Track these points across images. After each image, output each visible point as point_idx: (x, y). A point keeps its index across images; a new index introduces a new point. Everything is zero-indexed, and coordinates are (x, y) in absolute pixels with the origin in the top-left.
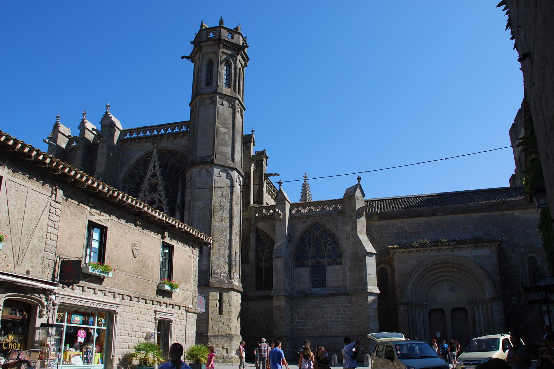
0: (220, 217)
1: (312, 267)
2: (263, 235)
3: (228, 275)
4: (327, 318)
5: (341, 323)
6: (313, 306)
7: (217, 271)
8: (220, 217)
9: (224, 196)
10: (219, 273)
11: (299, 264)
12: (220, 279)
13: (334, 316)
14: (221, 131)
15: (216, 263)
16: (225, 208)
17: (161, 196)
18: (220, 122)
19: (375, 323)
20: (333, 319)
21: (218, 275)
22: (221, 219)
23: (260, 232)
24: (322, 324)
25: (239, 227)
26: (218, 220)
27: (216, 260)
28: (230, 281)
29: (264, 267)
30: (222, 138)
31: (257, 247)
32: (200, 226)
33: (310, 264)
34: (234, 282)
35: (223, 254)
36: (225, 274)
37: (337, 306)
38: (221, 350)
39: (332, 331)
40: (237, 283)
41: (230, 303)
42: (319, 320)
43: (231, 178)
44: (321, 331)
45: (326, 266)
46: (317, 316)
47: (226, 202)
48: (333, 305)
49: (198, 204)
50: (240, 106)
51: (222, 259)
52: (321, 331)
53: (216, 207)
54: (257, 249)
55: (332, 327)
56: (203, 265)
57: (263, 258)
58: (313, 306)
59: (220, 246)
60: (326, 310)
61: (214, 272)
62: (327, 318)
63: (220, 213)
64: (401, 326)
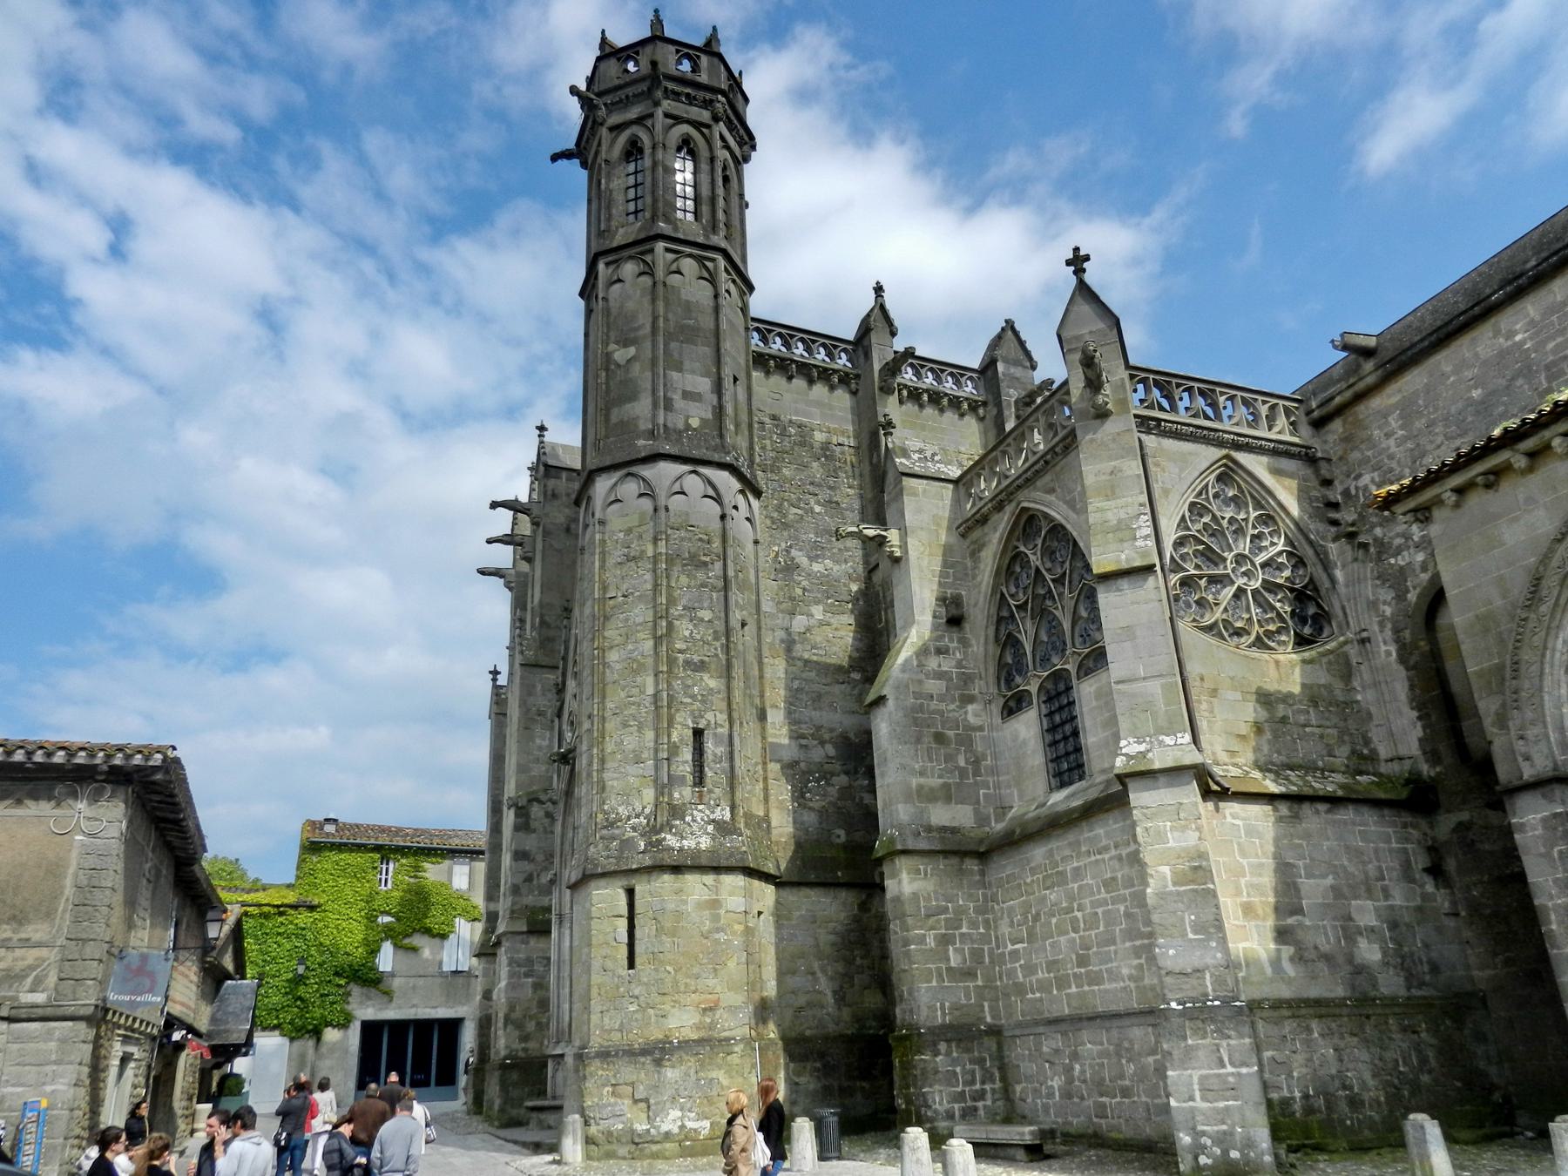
1: (1044, 702)
4: (1082, 925)
5: (1128, 944)
6: (1041, 876)
11: (1012, 704)
12: (622, 841)
13: (1104, 913)
18: (613, 338)
19: (1195, 932)
20: (1101, 929)
24: (1074, 957)
25: (716, 639)
33: (1033, 688)
36: (642, 818)
37: (1104, 860)
38: (626, 1108)
39: (1107, 986)
41: (660, 919)
42: (1062, 939)
43: (649, 493)
44: (1074, 989)
45: (1074, 681)
46: (1054, 921)
48: (1093, 858)
50: (688, 250)
51: (633, 769)
52: (1074, 989)
53: (612, 602)
55: (1103, 967)
58: (1041, 876)
59: (625, 725)
60: (1076, 886)
61: (607, 820)
62: (1082, 925)
64: (1554, 927)
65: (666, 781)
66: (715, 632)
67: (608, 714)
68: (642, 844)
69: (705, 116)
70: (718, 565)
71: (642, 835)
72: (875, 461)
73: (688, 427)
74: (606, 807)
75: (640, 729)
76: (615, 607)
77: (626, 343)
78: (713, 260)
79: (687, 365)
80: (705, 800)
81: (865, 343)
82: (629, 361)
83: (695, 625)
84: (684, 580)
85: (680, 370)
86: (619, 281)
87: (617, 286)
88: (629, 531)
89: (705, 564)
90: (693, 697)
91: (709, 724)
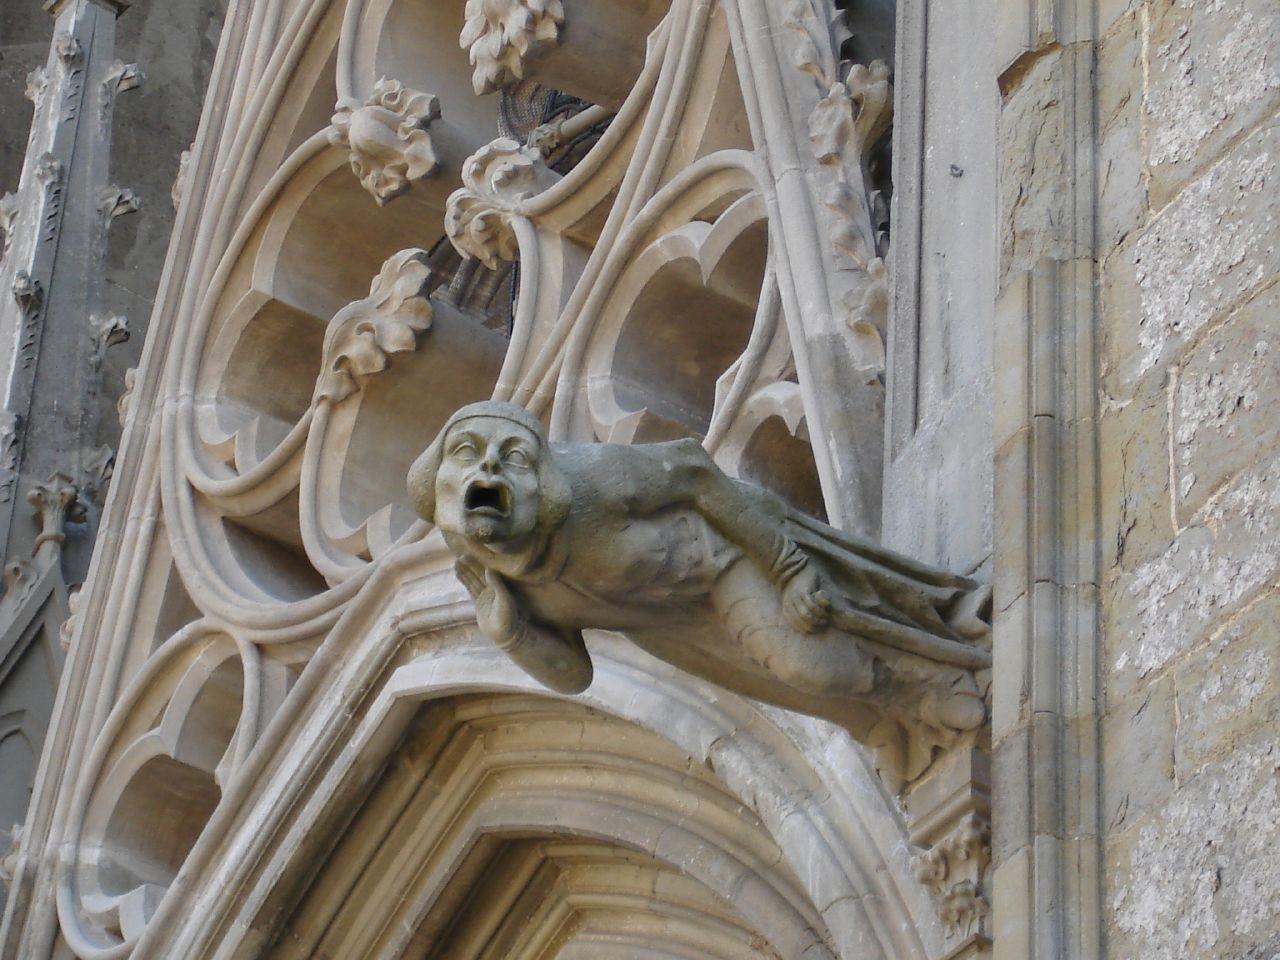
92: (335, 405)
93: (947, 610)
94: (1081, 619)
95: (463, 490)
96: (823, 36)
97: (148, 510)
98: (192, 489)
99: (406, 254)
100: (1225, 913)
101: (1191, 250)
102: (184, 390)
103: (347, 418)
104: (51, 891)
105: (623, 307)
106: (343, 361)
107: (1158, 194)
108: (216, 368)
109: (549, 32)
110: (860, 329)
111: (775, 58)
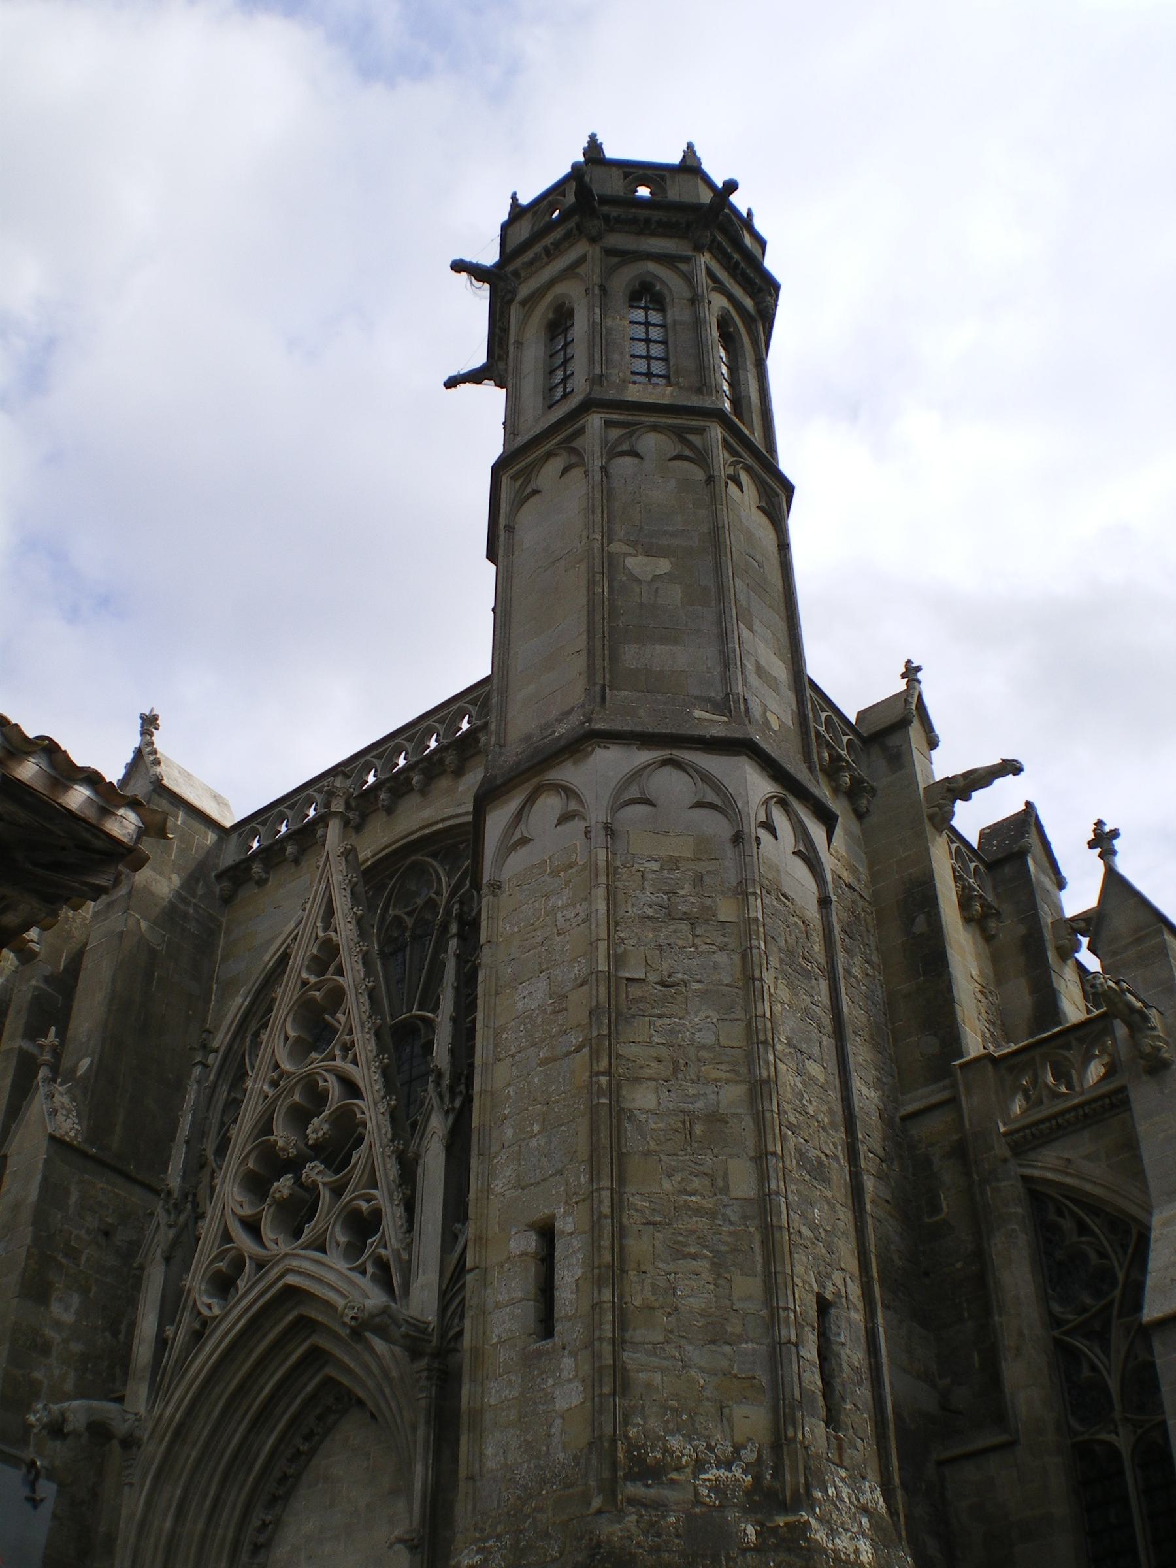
0: (664, 1052)
2: (1083, 1228)
3: (757, 1479)
7: (666, 1451)
8: (664, 1052)
9: (686, 917)
10: (679, 1469)
14: (636, 571)
15: (649, 1386)
16: (698, 986)
17: (355, 1056)
21: (672, 1481)
22: (675, 1062)
23: (1060, 1213)
25: (833, 1124)
26: (653, 1069)
27: (655, 1361)
28: (781, 1521)
29: (1126, 1455)
30: (642, 605)
31: (1055, 1322)
32: (534, 1143)
34: (819, 1534)
35: (704, 1314)
40: (864, 1546)
47: (703, 948)
49: (520, 1006)
50: (750, 461)
54: (1056, 1333)
56: (558, 1421)
57: (1110, 1382)
59: (678, 1254)
61: (641, 1460)
63: (659, 1022)
65: (797, 1396)
66: (831, 1112)
67: (632, 1219)
68: (750, 1530)
69: (749, 303)
70: (823, 985)
71: (746, 1511)
72: (920, 925)
73: (767, 723)
74: (632, 1432)
75: (718, 1267)
76: (642, 999)
77: (651, 552)
78: (778, 495)
79: (757, 626)
80: (847, 1463)
81: (893, 741)
82: (656, 578)
83: (803, 1083)
84: (784, 993)
85: (751, 630)
86: (634, 454)
87: (628, 460)
88: (674, 863)
89: (807, 975)
90: (813, 1227)
91: (838, 1294)
92: (270, 1206)
93: (426, 1329)
94: (479, 1390)
95: (350, 1316)
96: (396, 1173)
97: (221, 1209)
98: (232, 1210)
99: (290, 1176)
100: (506, 1458)
101: (504, 1323)
102: (231, 1184)
103: (272, 1210)
104: (195, 1293)
105: (344, 1214)
106: (274, 1197)
107: (498, 1306)
108: (238, 1180)
109: (327, 1136)
110: (404, 1249)
111: (387, 1176)
